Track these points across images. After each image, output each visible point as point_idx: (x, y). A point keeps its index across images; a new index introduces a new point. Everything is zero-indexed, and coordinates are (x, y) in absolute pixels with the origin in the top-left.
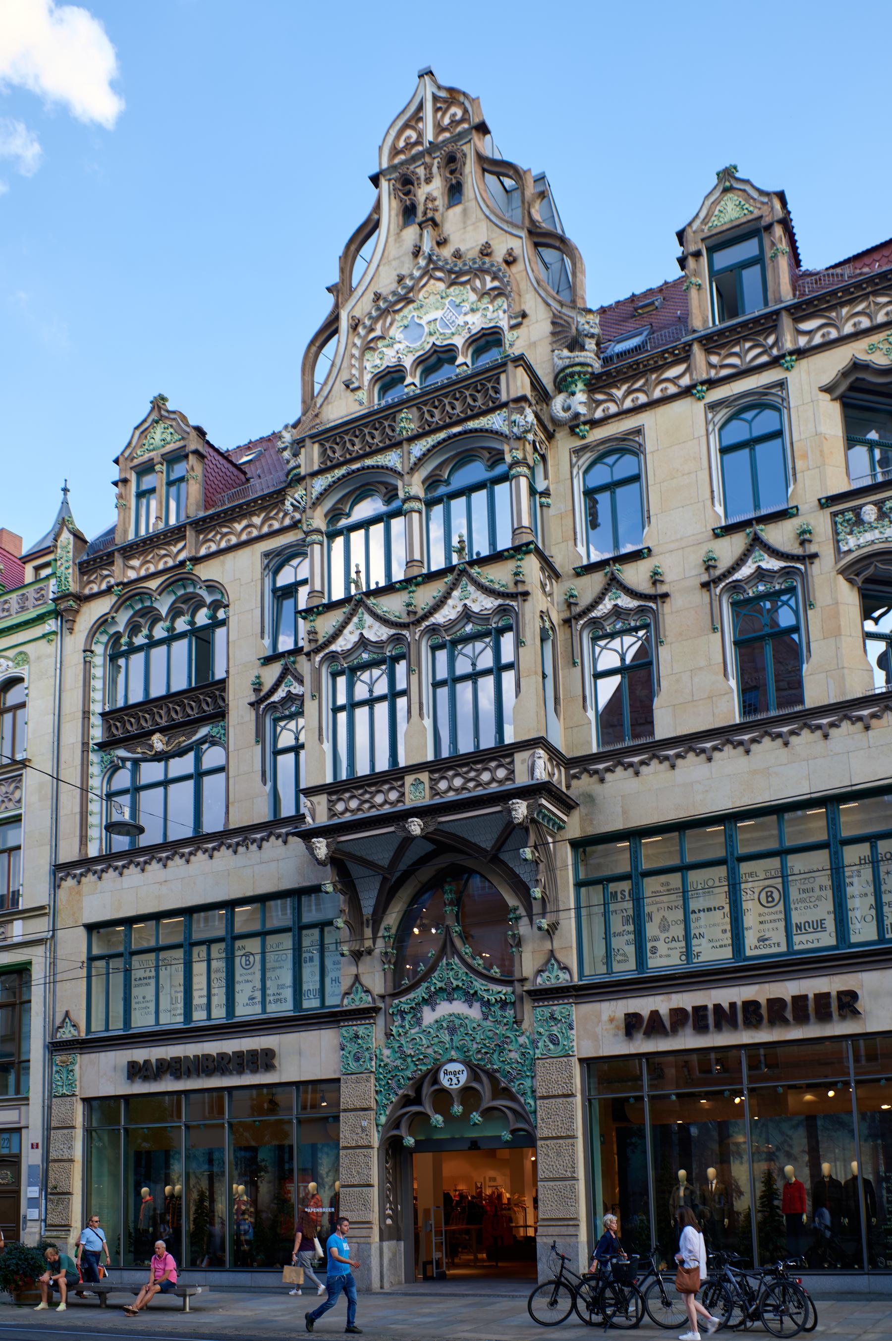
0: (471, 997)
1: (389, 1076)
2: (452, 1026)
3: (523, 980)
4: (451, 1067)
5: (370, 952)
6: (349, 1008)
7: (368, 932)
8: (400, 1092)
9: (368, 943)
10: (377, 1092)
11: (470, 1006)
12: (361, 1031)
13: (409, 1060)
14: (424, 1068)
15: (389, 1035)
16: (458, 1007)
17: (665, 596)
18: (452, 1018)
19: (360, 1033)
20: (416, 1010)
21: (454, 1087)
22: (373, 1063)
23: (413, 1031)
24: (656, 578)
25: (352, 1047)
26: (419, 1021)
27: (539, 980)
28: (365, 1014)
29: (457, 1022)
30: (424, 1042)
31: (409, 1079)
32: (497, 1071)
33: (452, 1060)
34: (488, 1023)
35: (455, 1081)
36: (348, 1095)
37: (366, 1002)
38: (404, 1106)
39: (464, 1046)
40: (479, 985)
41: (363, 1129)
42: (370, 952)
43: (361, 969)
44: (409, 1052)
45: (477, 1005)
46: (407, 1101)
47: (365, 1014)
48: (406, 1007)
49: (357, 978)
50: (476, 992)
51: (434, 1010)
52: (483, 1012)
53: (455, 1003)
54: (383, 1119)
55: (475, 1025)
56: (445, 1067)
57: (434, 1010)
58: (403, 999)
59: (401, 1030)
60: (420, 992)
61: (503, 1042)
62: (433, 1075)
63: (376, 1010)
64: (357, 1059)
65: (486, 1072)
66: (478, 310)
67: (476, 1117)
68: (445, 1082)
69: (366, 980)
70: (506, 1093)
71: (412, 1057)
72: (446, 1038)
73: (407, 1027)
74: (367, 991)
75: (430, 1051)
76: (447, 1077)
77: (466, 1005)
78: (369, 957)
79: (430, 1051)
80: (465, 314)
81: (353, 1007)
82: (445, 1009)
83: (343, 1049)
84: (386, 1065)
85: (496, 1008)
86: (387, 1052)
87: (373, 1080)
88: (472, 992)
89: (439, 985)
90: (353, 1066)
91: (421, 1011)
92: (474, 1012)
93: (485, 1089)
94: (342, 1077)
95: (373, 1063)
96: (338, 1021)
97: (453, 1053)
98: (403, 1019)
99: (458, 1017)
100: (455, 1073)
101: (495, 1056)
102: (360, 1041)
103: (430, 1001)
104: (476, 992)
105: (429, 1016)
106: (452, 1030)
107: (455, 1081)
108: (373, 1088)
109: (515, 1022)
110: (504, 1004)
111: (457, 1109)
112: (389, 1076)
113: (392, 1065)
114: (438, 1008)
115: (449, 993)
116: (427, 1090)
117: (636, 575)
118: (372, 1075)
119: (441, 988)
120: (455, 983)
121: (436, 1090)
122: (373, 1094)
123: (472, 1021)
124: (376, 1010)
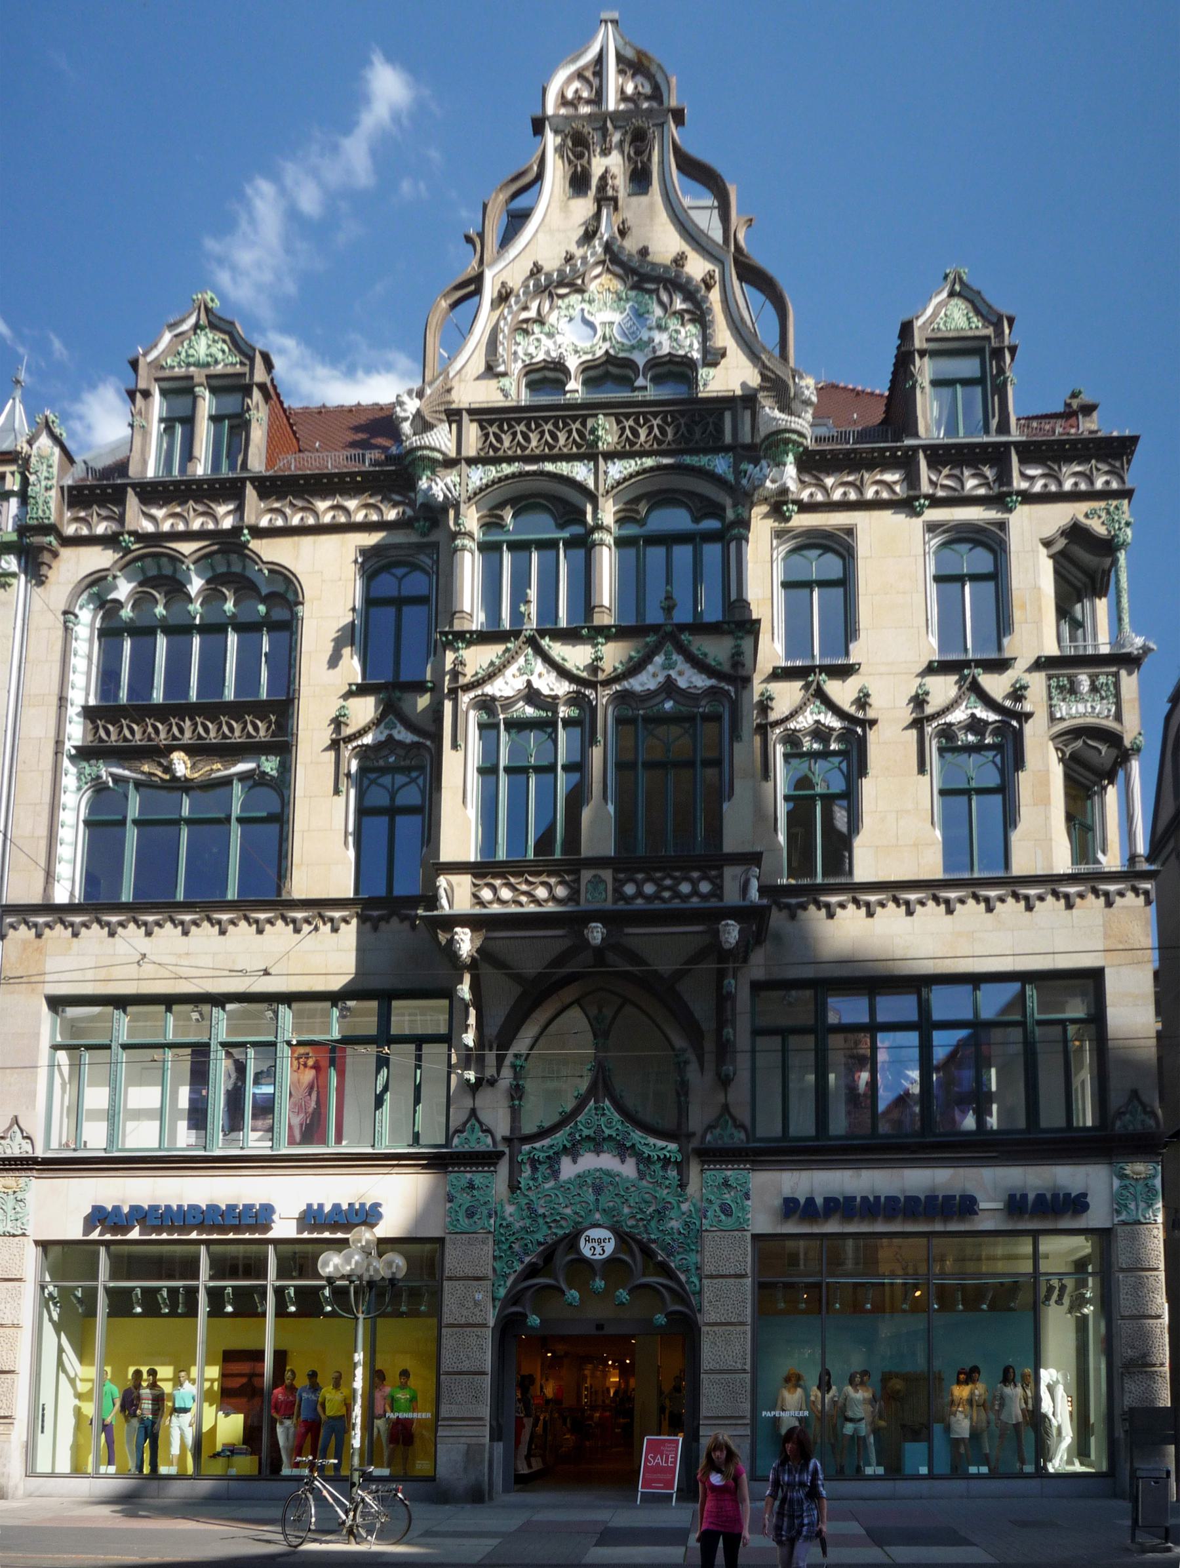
0: (623, 1150)
1: (512, 1239)
2: (599, 1183)
4: (595, 1233)
5: (492, 1083)
6: (460, 1149)
8: (527, 1260)
9: (490, 1072)
10: (495, 1258)
11: (623, 1162)
12: (478, 1179)
13: (541, 1220)
14: (561, 1232)
15: (514, 1187)
16: (607, 1161)
17: (873, 723)
19: (477, 1183)
20: (553, 1161)
21: (597, 1257)
22: (492, 1221)
23: (547, 1186)
24: (862, 701)
25: (465, 1199)
26: (555, 1174)
28: (488, 1159)
29: (606, 1179)
30: (561, 1200)
31: (540, 1244)
32: (654, 1241)
34: (644, 1183)
35: (599, 1250)
36: (454, 1260)
37: (486, 1144)
38: (526, 1279)
39: (614, 1209)
40: (637, 1136)
41: (477, 1304)
42: (492, 1083)
43: (479, 1103)
44: (541, 1211)
45: (631, 1163)
46: (532, 1271)
47: (488, 1159)
48: (542, 1155)
49: (473, 1113)
50: (633, 1145)
51: (575, 1162)
52: (639, 1171)
54: (502, 1292)
55: (629, 1185)
57: (575, 1162)
58: (537, 1145)
59: (531, 1183)
60: (560, 1137)
61: (665, 1208)
62: (572, 1240)
64: (470, 1214)
65: (639, 1242)
66: (666, 329)
67: (623, 1294)
68: (586, 1251)
69: (485, 1116)
70: (664, 1269)
71: (544, 1216)
74: (488, 1131)
75: (568, 1211)
76: (589, 1245)
77: (617, 1159)
79: (568, 1211)
80: (650, 329)
81: (466, 1148)
82: (589, 1161)
83: (451, 1201)
84: (508, 1226)
86: (510, 1209)
87: (491, 1243)
88: (628, 1144)
89: (586, 1132)
90: (464, 1222)
91: (558, 1163)
92: (628, 1169)
93: (637, 1261)
94: (448, 1237)
95: (492, 1221)
97: (597, 1216)
98: (534, 1169)
99: (608, 1173)
100: (599, 1241)
101: (653, 1224)
102: (475, 1192)
103: (572, 1151)
104: (633, 1145)
105: (568, 1169)
106: (598, 1190)
107: (599, 1250)
108: (491, 1253)
109: (680, 1186)
110: (666, 1162)
112: (512, 1239)
114: (580, 1160)
115: (597, 1143)
116: (562, 1259)
117: (842, 692)
118: (491, 1236)
119: (588, 1137)
120: (607, 1132)
121: (572, 1261)
122: (490, 1261)
123: (627, 1179)
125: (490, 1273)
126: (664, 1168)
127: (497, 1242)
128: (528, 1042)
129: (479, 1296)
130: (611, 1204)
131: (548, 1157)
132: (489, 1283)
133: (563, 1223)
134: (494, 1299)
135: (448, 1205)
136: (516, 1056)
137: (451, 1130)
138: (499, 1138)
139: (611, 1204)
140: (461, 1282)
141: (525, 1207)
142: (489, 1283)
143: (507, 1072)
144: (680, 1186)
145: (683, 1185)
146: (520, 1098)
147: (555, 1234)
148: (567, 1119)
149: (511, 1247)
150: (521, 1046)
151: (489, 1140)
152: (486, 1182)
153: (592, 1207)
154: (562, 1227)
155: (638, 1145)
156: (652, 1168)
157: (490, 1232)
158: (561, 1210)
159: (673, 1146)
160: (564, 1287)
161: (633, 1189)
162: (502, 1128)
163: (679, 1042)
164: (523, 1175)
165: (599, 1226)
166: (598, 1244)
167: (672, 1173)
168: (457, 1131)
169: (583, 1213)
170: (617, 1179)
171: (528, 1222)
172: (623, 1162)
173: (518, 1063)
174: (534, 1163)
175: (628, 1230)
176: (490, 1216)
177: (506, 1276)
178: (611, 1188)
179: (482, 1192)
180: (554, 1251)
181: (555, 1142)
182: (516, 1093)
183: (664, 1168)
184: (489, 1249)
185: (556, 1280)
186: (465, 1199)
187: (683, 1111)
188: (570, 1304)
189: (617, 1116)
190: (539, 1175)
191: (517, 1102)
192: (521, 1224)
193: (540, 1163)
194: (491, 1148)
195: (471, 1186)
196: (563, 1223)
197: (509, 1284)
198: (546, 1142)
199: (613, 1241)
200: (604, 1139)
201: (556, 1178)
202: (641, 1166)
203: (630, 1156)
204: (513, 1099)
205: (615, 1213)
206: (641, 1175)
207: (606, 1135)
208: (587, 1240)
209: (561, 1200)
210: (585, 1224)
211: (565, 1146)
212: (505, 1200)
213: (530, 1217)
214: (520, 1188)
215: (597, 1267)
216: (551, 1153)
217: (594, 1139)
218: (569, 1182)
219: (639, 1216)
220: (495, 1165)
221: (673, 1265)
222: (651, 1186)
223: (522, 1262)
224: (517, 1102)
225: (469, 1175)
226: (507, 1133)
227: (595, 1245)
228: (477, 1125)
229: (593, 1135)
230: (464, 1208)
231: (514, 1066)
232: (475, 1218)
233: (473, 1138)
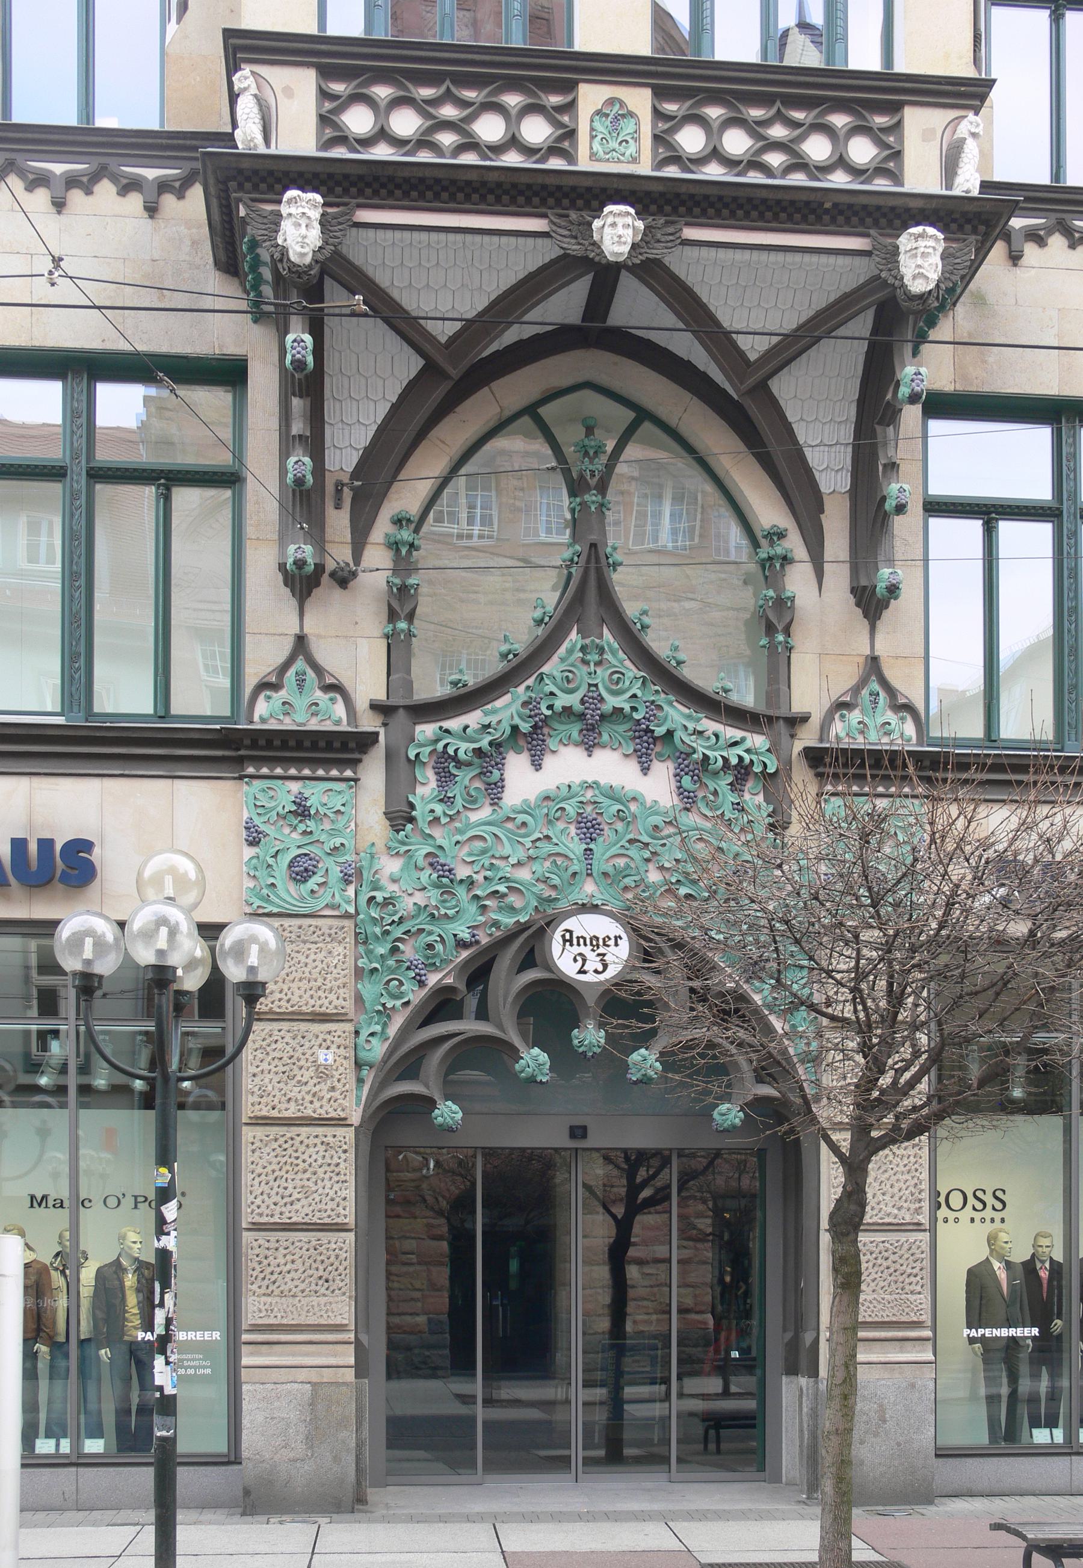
0: (648, 743)
1: (398, 932)
3: (795, 722)
5: (343, 579)
6: (273, 725)
7: (339, 522)
8: (433, 979)
9: (340, 553)
10: (359, 973)
11: (645, 770)
12: (316, 794)
13: (461, 892)
14: (508, 921)
15: (400, 817)
16: (611, 767)
18: (589, 794)
19: (313, 802)
20: (489, 759)
22: (351, 891)
23: (474, 817)
25: (289, 840)
26: (495, 790)
27: (838, 728)
31: (462, 944)
33: (591, 908)
37: (334, 716)
39: (624, 873)
40: (676, 715)
42: (343, 579)
44: (462, 872)
48: (464, 749)
49: (301, 642)
50: (670, 733)
51: (537, 766)
53: (600, 754)
54: (377, 1050)
55: (657, 820)
56: (569, 924)
57: (537, 766)
59: (439, 809)
63: (364, 742)
64: (301, 872)
68: (565, 962)
69: (326, 653)
71: (470, 883)
72: (577, 848)
73: (459, 802)
74: (335, 688)
75: (524, 875)
78: (338, 593)
79: (524, 875)
81: (288, 724)
82: (569, 766)
83: (253, 843)
84: (388, 902)
85: (723, 783)
86: (391, 866)
87: (350, 939)
88: (660, 731)
91: (500, 765)
92: (658, 786)
95: (351, 891)
96: (241, 761)
97: (590, 887)
98: (445, 777)
99: (611, 793)
100: (594, 942)
102: (311, 825)
103: (533, 738)
104: (670, 733)
105: (522, 781)
106: (589, 829)
108: (350, 962)
110: (742, 772)
111: (590, 1036)
112: (398, 932)
113: (407, 905)
114: (548, 761)
118: (348, 924)
119: (567, 710)
120: (612, 702)
123: (653, 809)
124: (364, 742)
125: (349, 1006)
126: (736, 786)
127: (362, 939)
128: (423, 489)
129: (325, 1057)
130: (621, 862)
131: (479, 752)
132: (349, 1027)
133: (512, 899)
134: (358, 1065)
135: (249, 852)
136: (399, 522)
137: (250, 682)
138: (362, 703)
139: (621, 862)
140: (285, 1026)
141: (421, 862)
142: (349, 1027)
143: (377, 557)
144: (772, 827)
145: (778, 825)
146: (410, 617)
147: (496, 924)
148: (519, 668)
149: (394, 950)
150: (408, 496)
151: (339, 710)
152: (337, 802)
153: (576, 867)
154: (512, 909)
155: (679, 734)
156: (712, 785)
157: (347, 916)
158: (507, 870)
159: (759, 741)
160: (517, 1041)
161: (671, 830)
162: (369, 683)
163: (768, 510)
164: (420, 790)
165: (594, 909)
166: (591, 951)
167: (754, 798)
168: (264, 686)
169: (556, 881)
170: (633, 807)
171: (433, 896)
172: (645, 770)
173: (406, 535)
174: (446, 764)
175: (659, 920)
176: (348, 882)
177: (385, 1013)
178: (620, 826)
179: (327, 826)
180: (492, 961)
181: (493, 719)
182: (401, 604)
183: (736, 786)
184: (341, 954)
185: (500, 1026)
186: (289, 840)
187: (776, 666)
188: (532, 1080)
189: (631, 671)
190: (456, 791)
191: (402, 625)
192: (420, 898)
193: (459, 764)
194: (344, 727)
195: (302, 811)
196: (512, 899)
197: (392, 1031)
198: (473, 719)
199: (625, 945)
200: (602, 717)
201: (496, 801)
202: (687, 781)
203: (660, 757)
204: (392, 616)
205: (629, 881)
206: (688, 800)
207: (607, 708)
208: (568, 939)
209: (507, 850)
210: (563, 905)
211: (515, 729)
212: (380, 846)
213: (437, 886)
214: (412, 820)
215: (591, 999)
216: (484, 743)
217: (581, 716)
218: (526, 809)
219: (683, 891)
220: (354, 763)
221: (757, 998)
222: (708, 825)
223: (422, 984)
224: (402, 625)
225: (295, 787)
226: (381, 695)
227: (586, 950)
228: (311, 674)
229: (578, 707)
230: (285, 860)
231: (394, 546)
232: (311, 884)
233: (300, 703)
